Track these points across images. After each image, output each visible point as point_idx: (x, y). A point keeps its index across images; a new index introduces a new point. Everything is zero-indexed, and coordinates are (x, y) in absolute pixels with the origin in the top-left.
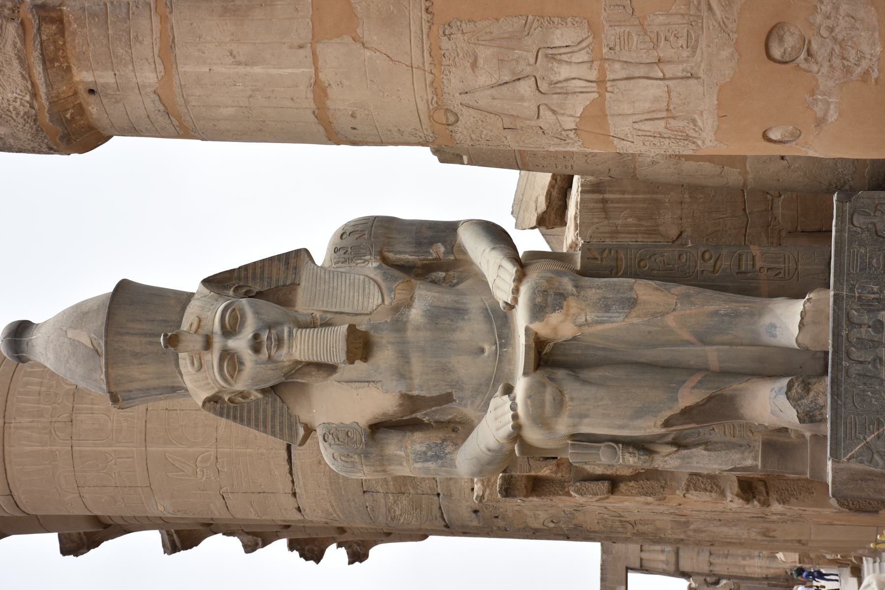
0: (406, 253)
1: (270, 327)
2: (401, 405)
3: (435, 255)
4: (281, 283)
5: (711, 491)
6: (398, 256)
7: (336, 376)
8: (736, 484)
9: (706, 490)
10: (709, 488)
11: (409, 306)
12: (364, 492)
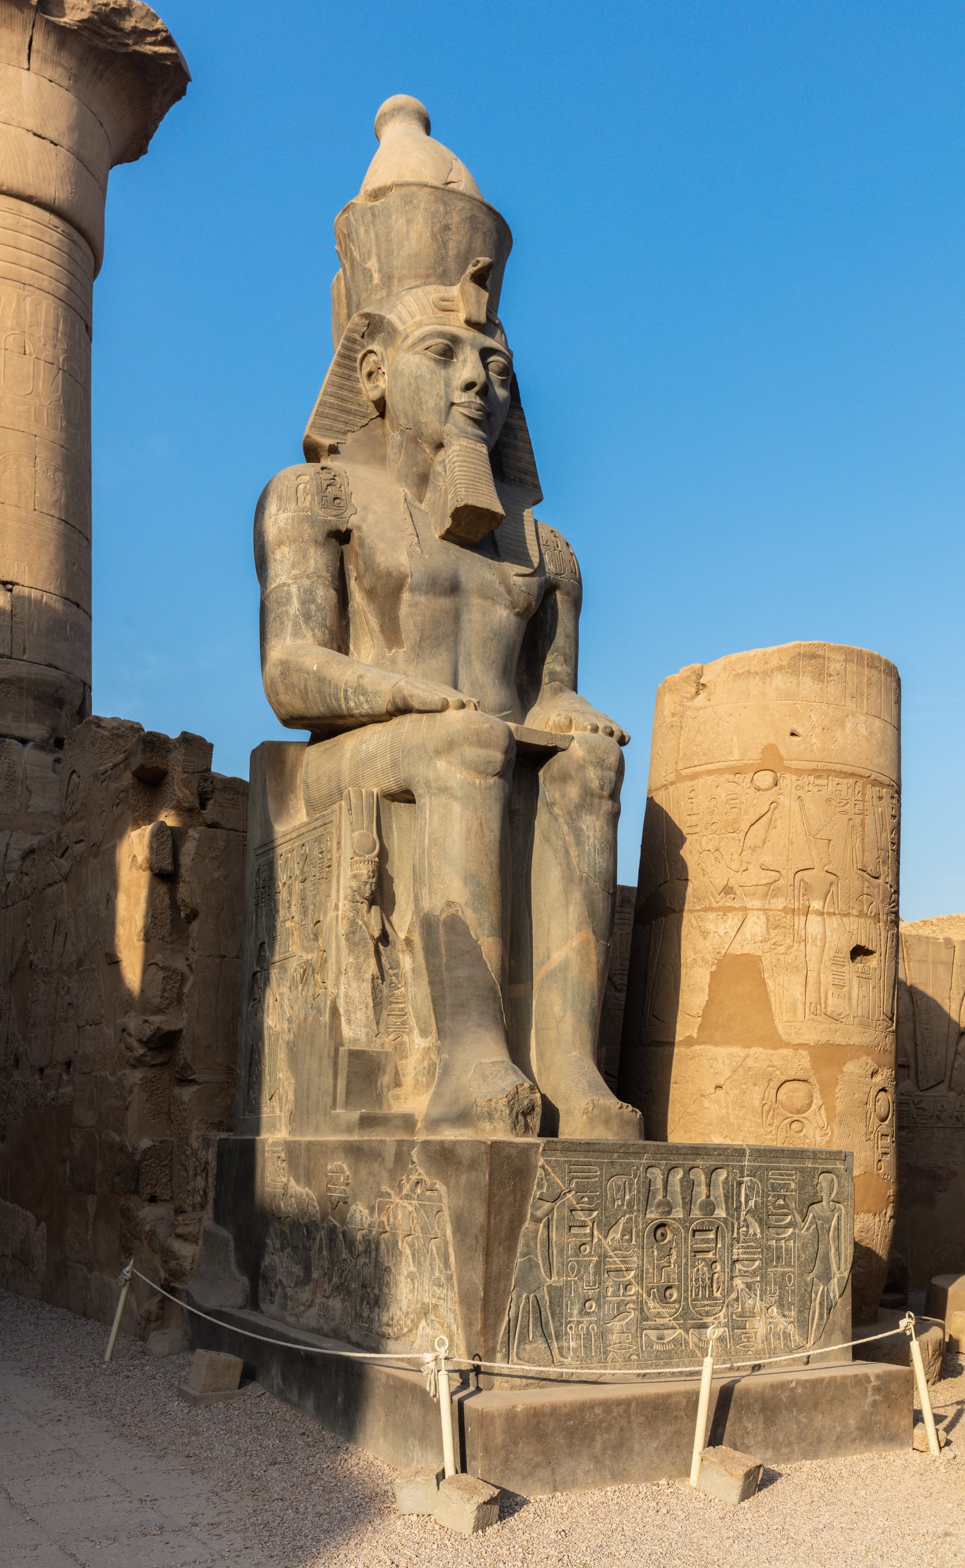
5: (162, 997)
9: (164, 991)
10: (166, 995)
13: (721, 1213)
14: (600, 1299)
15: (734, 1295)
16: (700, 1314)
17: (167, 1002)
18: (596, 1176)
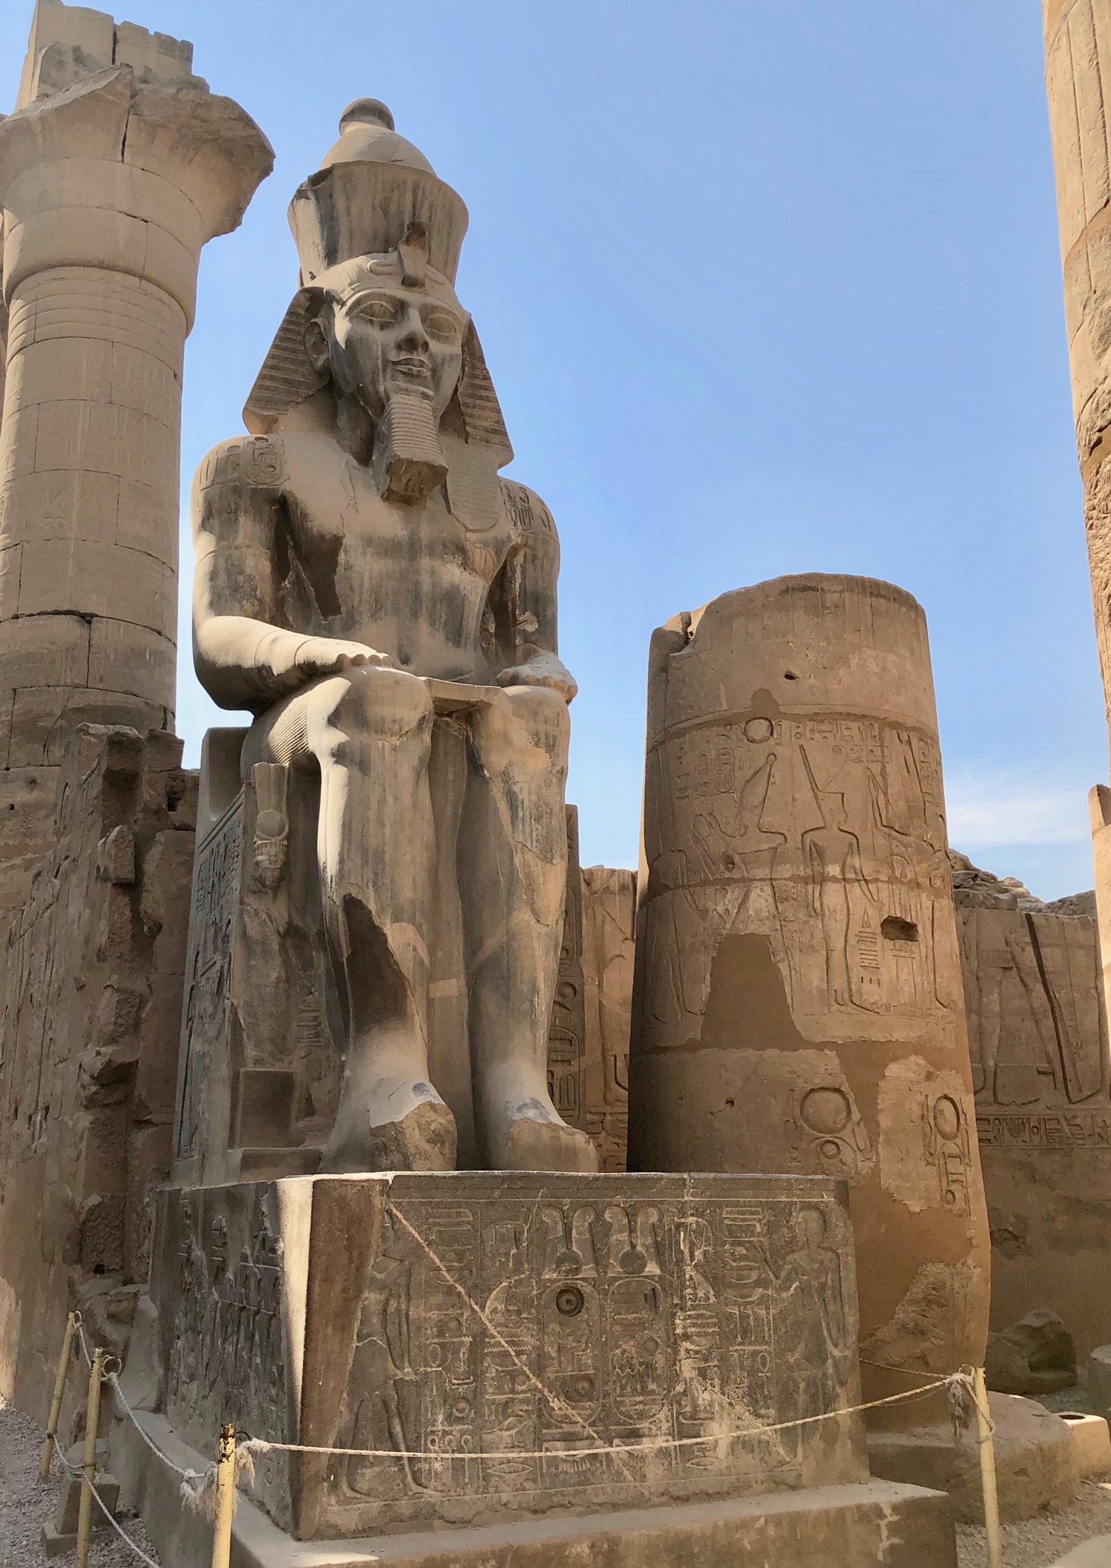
0: (524, 578)
1: (434, 371)
2: (322, 537)
3: (521, 618)
4: (468, 420)
6: (518, 569)
7: (355, 462)
8: (127, 1060)
9: (118, 1016)
11: (466, 565)
12: (15, 690)
13: (652, 1268)
14: (474, 1399)
15: (680, 1388)
16: (630, 1417)
17: (122, 1029)
18: (468, 1223)
